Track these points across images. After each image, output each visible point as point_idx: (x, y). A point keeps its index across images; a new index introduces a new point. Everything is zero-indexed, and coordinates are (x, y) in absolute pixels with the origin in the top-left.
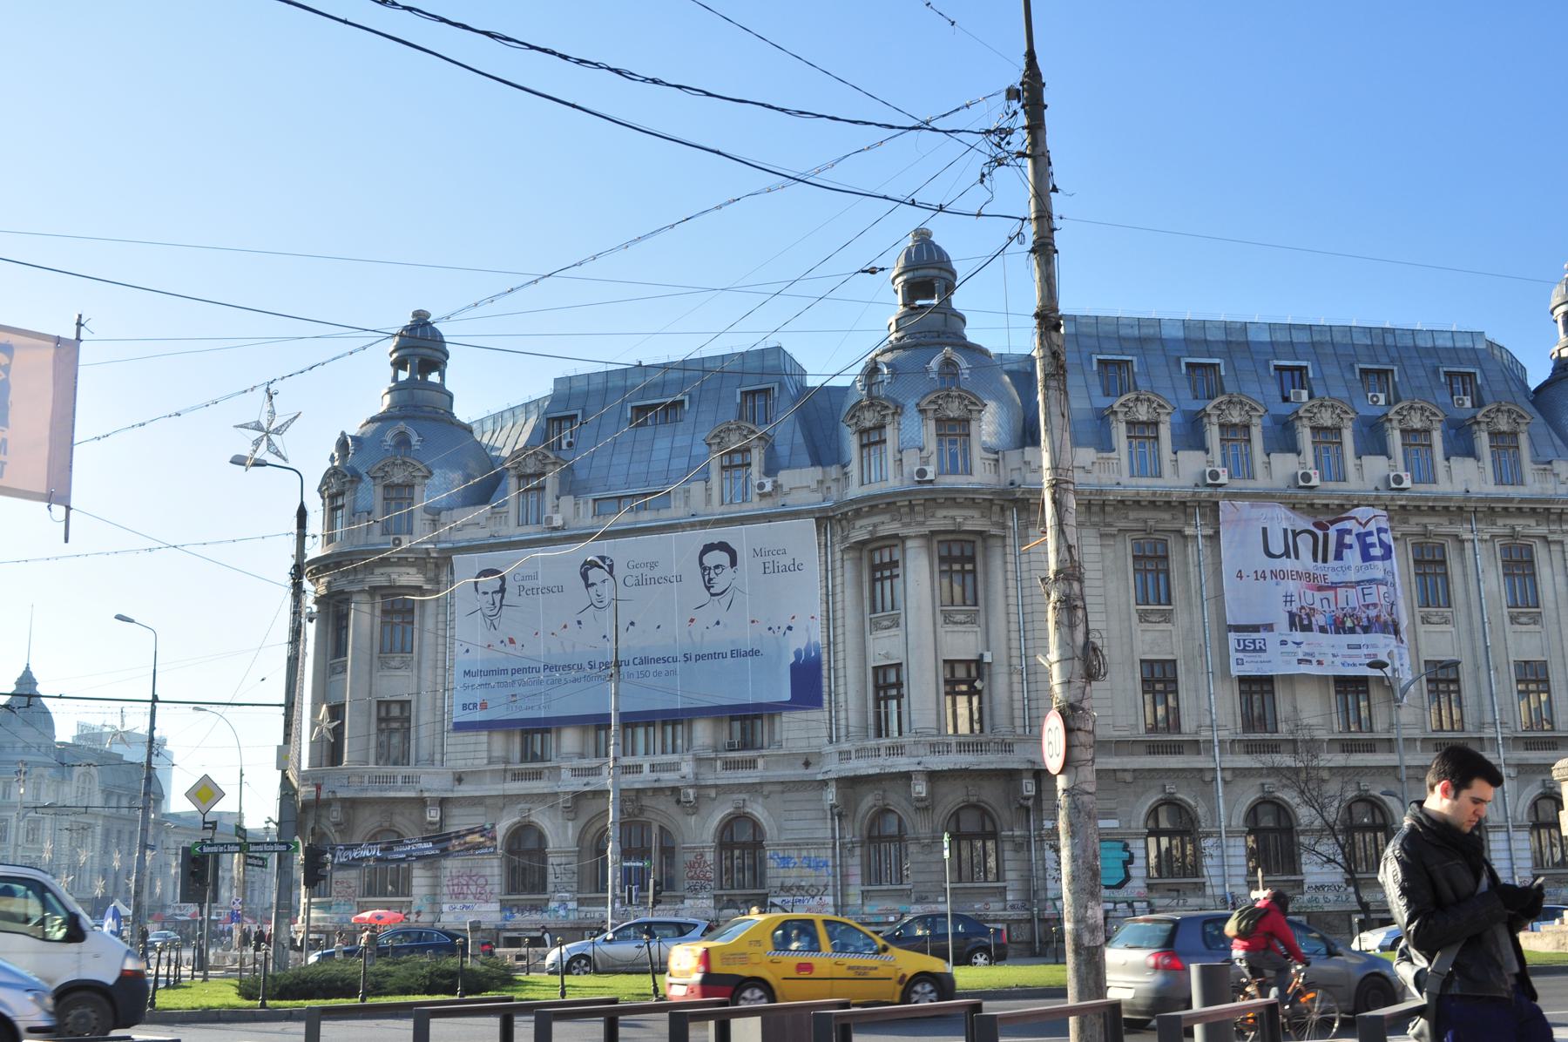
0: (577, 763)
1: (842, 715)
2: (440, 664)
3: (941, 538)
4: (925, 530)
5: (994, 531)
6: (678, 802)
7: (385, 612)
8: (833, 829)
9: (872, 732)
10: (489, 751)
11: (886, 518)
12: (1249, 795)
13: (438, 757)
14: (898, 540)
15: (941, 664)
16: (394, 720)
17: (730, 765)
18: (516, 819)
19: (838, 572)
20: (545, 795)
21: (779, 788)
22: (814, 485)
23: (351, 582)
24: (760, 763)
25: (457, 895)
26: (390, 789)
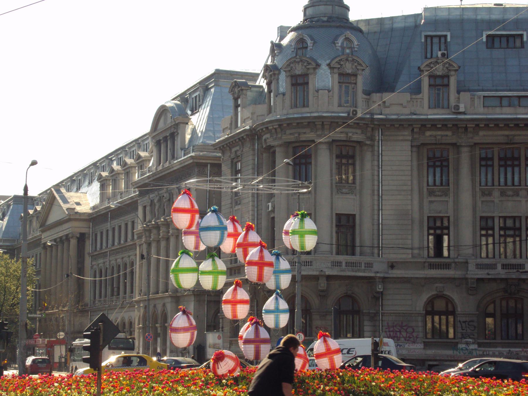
2: (376, 193)
20: (454, 279)
26: (359, 271)
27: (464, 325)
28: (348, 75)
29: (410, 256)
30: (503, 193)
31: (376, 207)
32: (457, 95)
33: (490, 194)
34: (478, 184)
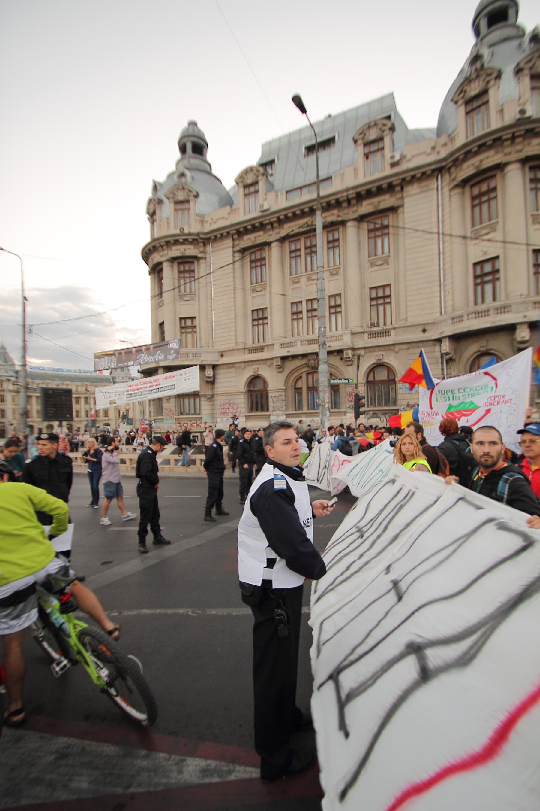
0: (282, 341)
1: (449, 297)
2: (209, 296)
6: (341, 359)
7: (180, 272)
8: (443, 369)
9: (472, 304)
10: (236, 339)
13: (211, 344)
16: (187, 325)
17: (373, 335)
18: (252, 373)
19: (447, 205)
21: (405, 346)
22: (429, 150)
23: (162, 256)
24: (392, 332)
25: (224, 414)
26: (186, 360)
27: (274, 399)
28: (182, 202)
29: (234, 344)
30: (309, 279)
31: (210, 309)
32: (265, 197)
33: (298, 282)
34: (288, 274)
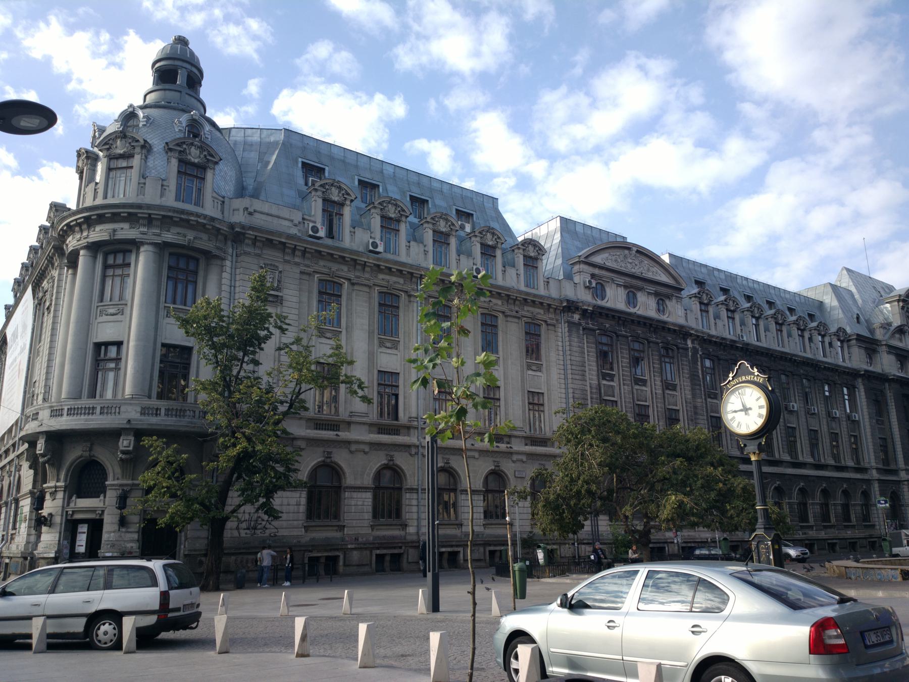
3: (172, 250)
4: (158, 240)
5: (217, 253)
11: (126, 226)
12: (378, 460)
14: (133, 245)
15: (159, 346)
